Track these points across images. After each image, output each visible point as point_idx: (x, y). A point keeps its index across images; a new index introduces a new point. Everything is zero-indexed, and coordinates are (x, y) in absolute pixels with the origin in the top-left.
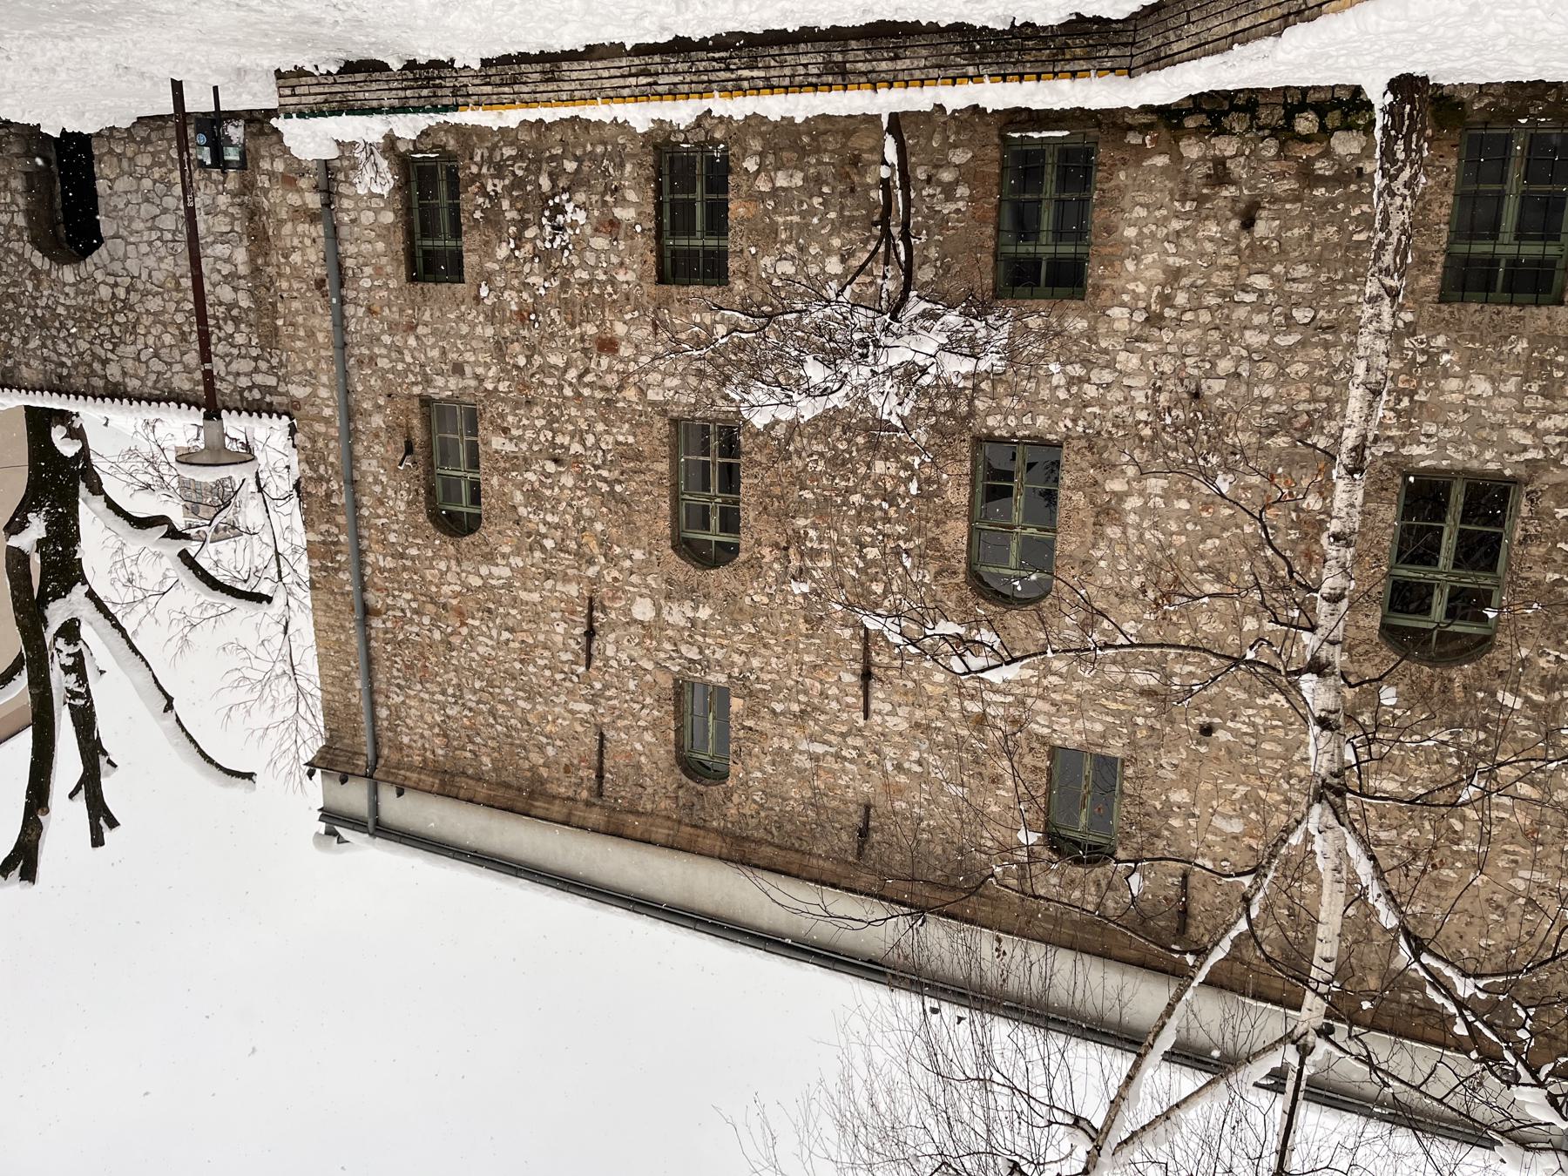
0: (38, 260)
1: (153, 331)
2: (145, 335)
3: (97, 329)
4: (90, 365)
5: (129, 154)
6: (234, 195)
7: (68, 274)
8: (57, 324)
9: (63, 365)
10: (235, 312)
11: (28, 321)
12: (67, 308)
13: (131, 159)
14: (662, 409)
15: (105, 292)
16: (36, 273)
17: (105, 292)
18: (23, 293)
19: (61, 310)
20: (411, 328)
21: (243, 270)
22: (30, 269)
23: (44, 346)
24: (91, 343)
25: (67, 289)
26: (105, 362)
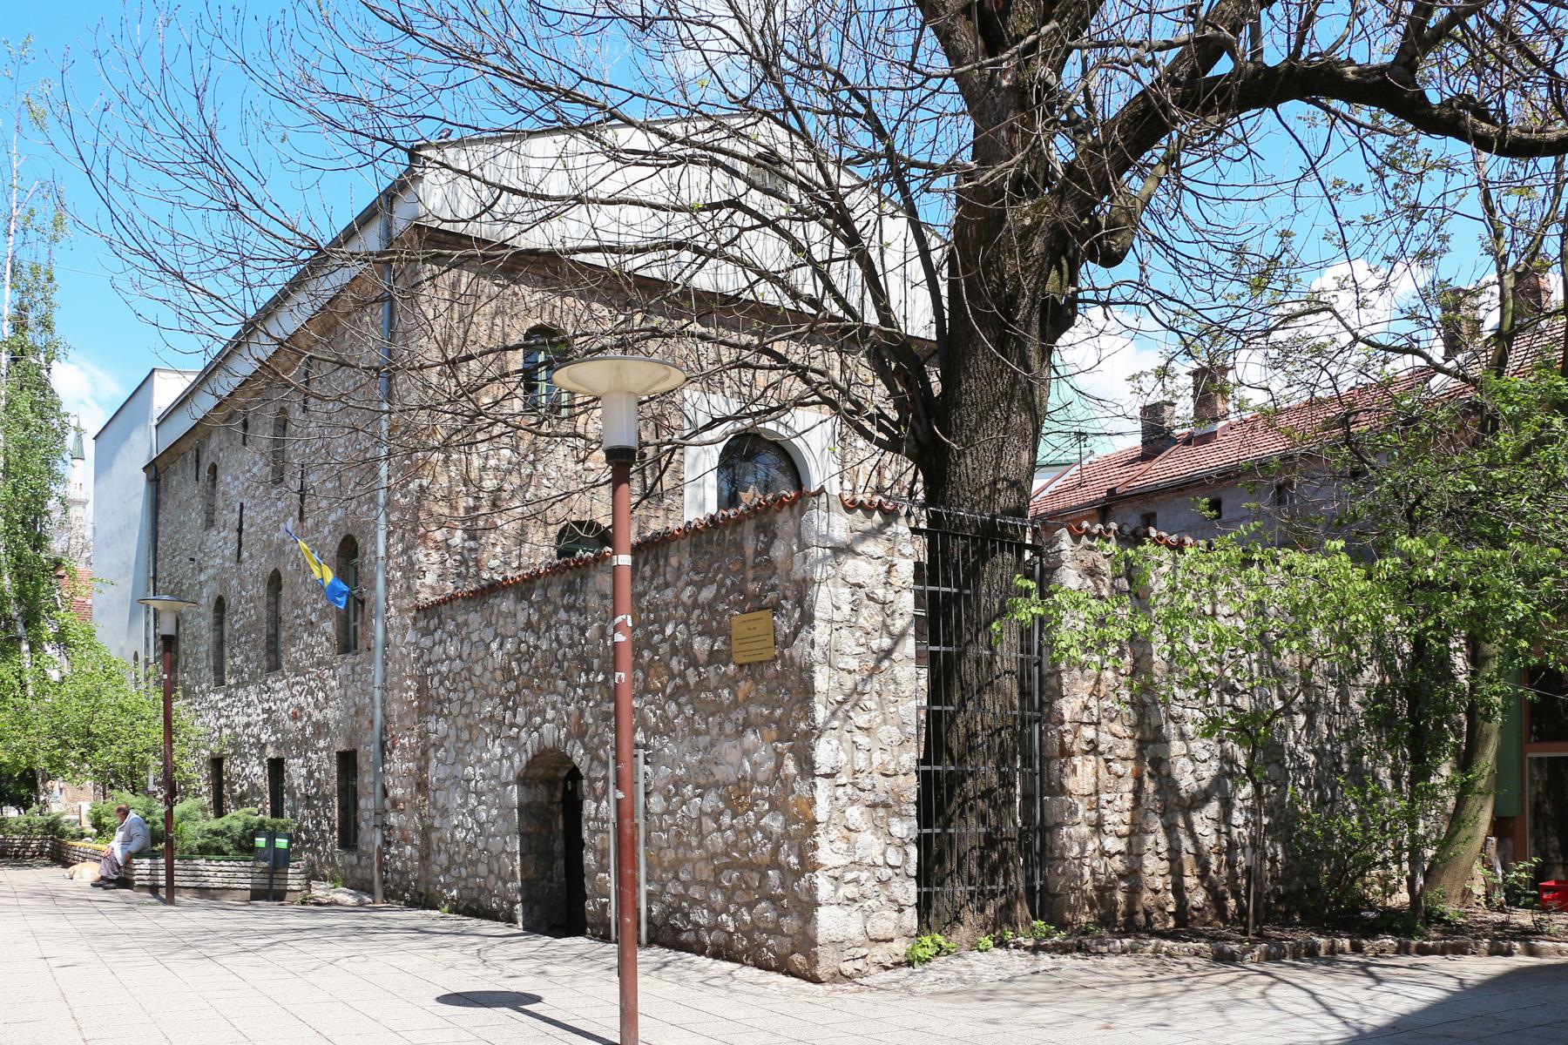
0: (578, 754)
1: (488, 675)
2: (495, 669)
3: (531, 667)
4: (542, 616)
5: (492, 878)
6: (431, 826)
7: (550, 733)
8: (566, 664)
9: (569, 608)
10: (438, 708)
11: (596, 662)
12: (556, 692)
13: (491, 872)
14: (285, 677)
15: (520, 720)
16: (580, 733)
17: (520, 720)
18: (597, 704)
19: (561, 684)
20: (357, 713)
21: (432, 751)
22: (586, 739)
23: (583, 630)
24: (536, 647)
25: (550, 714)
26: (529, 626)
